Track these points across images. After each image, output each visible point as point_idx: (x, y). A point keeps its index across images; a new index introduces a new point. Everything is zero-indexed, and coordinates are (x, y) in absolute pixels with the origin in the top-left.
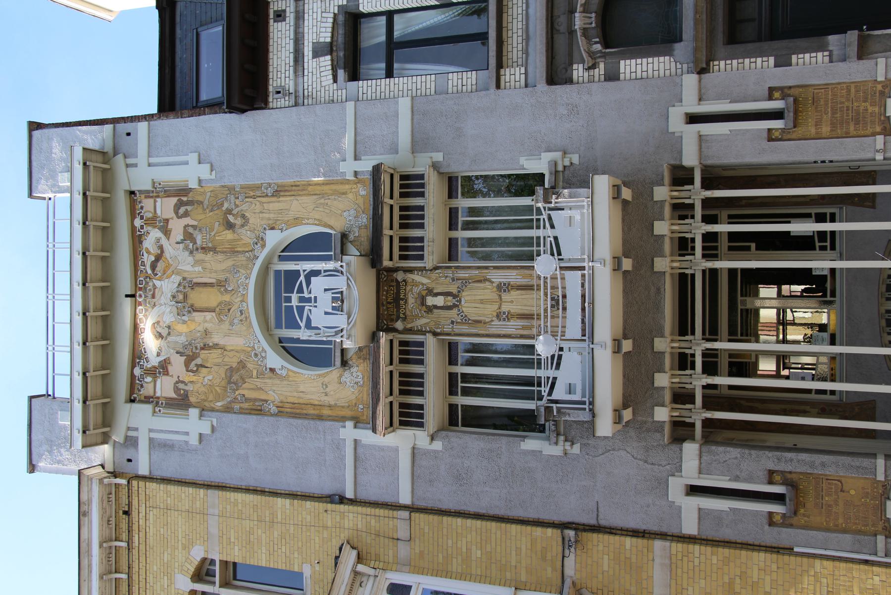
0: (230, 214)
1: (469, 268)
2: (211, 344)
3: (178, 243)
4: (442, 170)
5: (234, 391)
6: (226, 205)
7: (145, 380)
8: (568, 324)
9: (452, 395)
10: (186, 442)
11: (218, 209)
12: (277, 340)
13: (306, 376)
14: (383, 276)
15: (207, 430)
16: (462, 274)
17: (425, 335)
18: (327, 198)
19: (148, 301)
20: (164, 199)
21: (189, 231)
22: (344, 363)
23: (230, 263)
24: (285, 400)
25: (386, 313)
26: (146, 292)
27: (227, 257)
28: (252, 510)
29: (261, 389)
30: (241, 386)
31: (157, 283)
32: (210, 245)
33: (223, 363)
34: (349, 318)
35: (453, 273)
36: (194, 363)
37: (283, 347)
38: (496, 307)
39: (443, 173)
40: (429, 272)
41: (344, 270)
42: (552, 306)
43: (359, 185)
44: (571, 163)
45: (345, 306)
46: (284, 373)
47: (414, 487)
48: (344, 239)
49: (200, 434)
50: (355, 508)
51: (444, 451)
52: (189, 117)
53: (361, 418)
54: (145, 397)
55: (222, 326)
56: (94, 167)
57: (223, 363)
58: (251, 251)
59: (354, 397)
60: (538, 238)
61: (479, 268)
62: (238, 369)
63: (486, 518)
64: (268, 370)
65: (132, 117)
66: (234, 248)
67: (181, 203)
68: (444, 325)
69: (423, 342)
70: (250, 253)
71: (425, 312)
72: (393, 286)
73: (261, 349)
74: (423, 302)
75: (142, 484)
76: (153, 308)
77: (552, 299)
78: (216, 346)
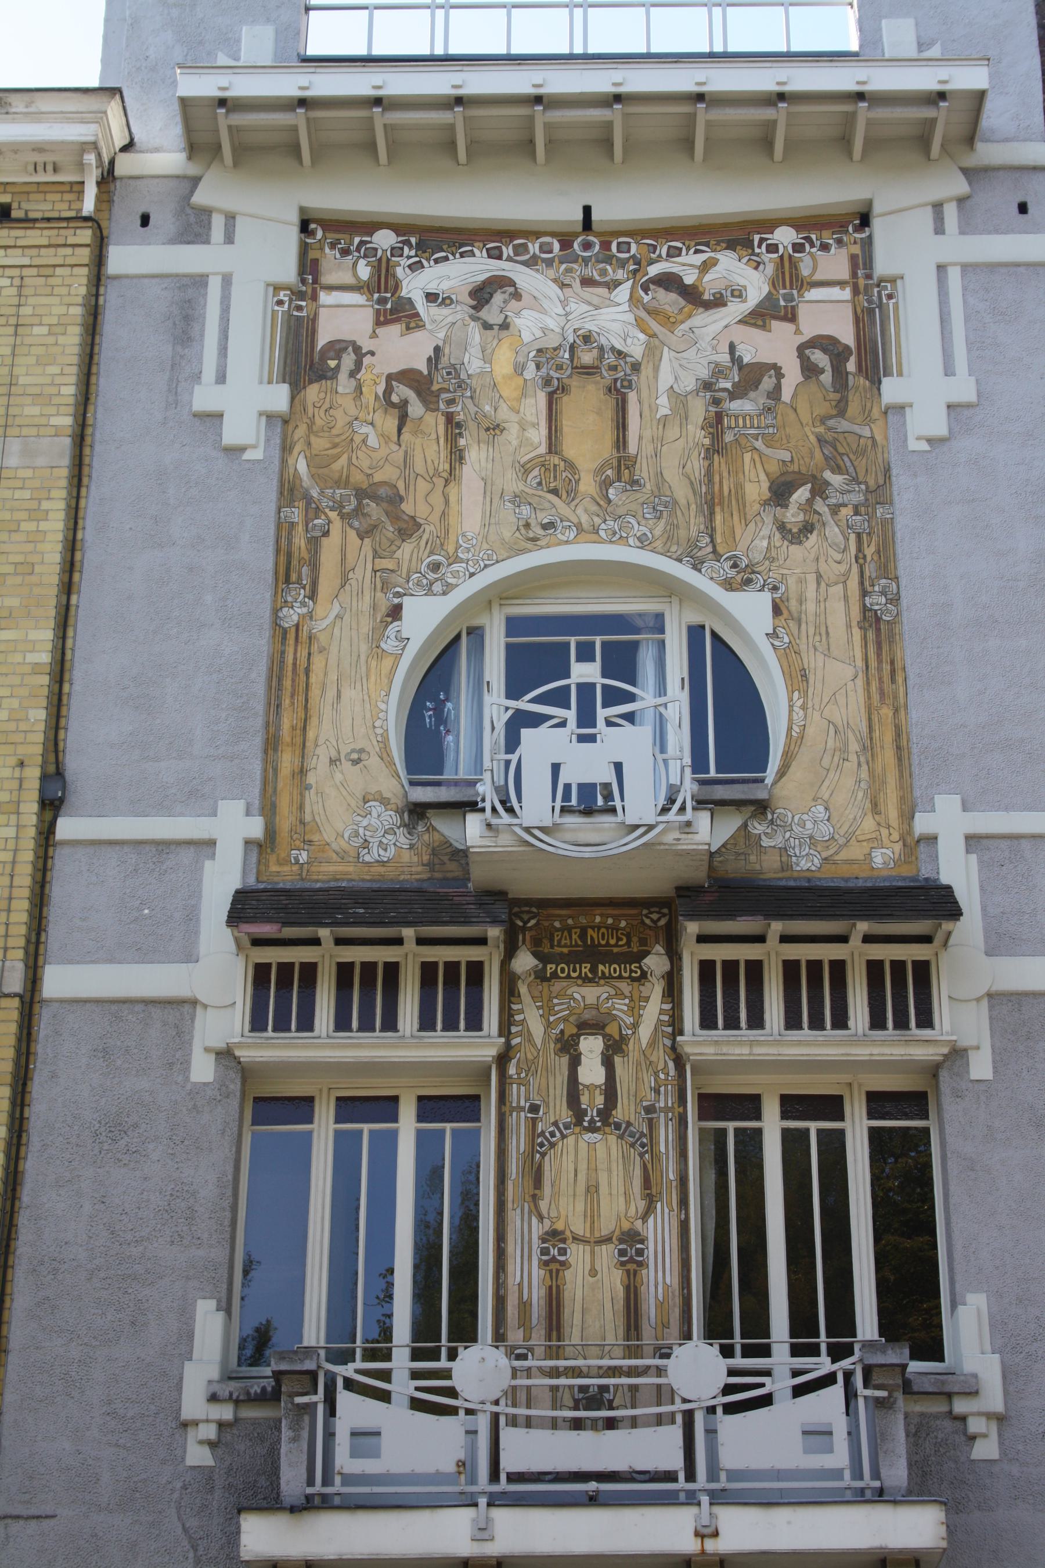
0: (814, 492)
1: (683, 1154)
2: (462, 442)
3: (732, 347)
4: (944, 1075)
5: (339, 507)
6: (836, 480)
7: (362, 262)
8: (541, 1436)
9: (337, 1106)
10: (197, 377)
11: (826, 458)
12: (476, 622)
13: (383, 706)
14: (655, 916)
15: (231, 436)
16: (665, 1136)
17: (500, 1035)
18: (862, 759)
19: (575, 266)
21: (766, 379)
22: (417, 812)
23: (682, 492)
24: (315, 648)
25: (557, 924)
26: (598, 261)
28: (20, 558)
29: (345, 581)
30: (351, 527)
31: (623, 293)
32: (728, 437)
33: (412, 475)
35: (666, 1110)
36: (410, 394)
37: (458, 637)
38: (579, 1227)
39: (935, 1076)
40: (668, 1042)
41: (672, 816)
42: (583, 1389)
43: (898, 847)
44: (973, 1438)
45: (570, 820)
46: (390, 645)
47: (88, 1005)
48: (753, 808)
49: (220, 416)
50: (31, 844)
51: (189, 1087)
53: (273, 858)
54: (315, 262)
55: (510, 474)
56: (933, 121)
57: (412, 475)
58: (715, 551)
59: (328, 835)
60: (765, 1351)
61: (683, 1180)
62: (398, 518)
63: (9, 1203)
64: (396, 601)
66: (721, 503)
67: (839, 355)
69: (480, 1029)
70: (709, 549)
71: (562, 1032)
72: (628, 944)
74: (587, 1027)
75: (84, 255)
76: (555, 281)
77: (604, 1389)
78: (457, 456)
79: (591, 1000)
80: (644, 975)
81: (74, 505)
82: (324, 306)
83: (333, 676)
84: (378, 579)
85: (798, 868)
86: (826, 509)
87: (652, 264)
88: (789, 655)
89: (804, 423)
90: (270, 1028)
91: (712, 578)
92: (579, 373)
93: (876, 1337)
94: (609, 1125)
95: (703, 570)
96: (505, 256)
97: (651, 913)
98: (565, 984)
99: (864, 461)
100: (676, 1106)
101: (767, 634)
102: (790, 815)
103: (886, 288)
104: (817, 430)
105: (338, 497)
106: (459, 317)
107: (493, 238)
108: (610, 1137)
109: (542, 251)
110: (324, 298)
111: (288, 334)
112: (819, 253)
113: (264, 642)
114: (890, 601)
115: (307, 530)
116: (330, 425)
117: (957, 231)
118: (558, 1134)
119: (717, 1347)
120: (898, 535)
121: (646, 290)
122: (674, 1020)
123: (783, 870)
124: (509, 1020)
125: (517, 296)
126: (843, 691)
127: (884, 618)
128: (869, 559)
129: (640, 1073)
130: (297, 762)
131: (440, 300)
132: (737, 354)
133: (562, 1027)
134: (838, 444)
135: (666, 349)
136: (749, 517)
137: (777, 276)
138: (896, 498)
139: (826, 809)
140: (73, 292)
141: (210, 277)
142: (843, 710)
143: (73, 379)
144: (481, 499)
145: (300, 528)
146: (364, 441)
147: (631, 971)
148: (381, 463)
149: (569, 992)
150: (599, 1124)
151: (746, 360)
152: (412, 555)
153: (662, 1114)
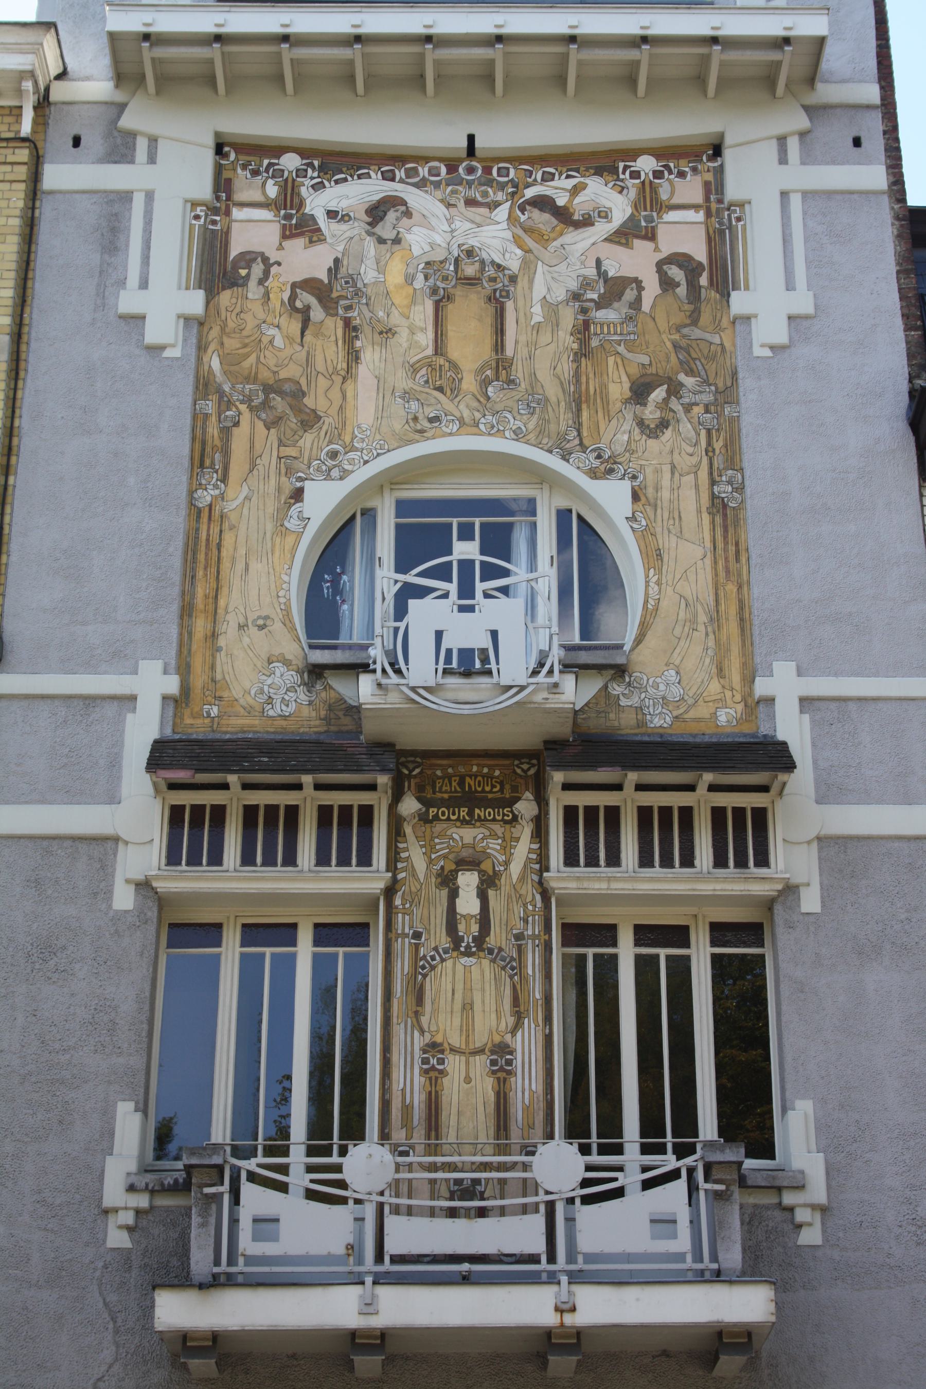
0: (669, 393)
1: (548, 976)
2: (358, 344)
3: (598, 262)
4: (778, 909)
5: (248, 400)
6: (689, 381)
7: (270, 182)
8: (420, 1223)
9: (242, 931)
10: (122, 283)
11: (681, 362)
12: (369, 504)
13: (286, 578)
14: (525, 767)
15: (153, 334)
16: (532, 960)
17: (388, 871)
19: (460, 188)
20: (701, 232)
21: (628, 291)
22: (316, 672)
23: (552, 391)
24: (226, 526)
25: (439, 773)
26: (481, 184)
27: (566, 386)
29: (253, 466)
30: (259, 418)
31: (502, 213)
32: (594, 343)
34: (426, 688)
35: (534, 937)
37: (353, 518)
38: (456, 1040)
39: (770, 909)
40: (536, 878)
41: (541, 678)
42: (458, 1182)
43: (740, 707)
44: (800, 1226)
45: (453, 681)
46: (292, 524)
47: (22, 840)
49: (143, 317)
51: (111, 914)
52: (900, 290)
53: (187, 712)
54: (229, 181)
55: (401, 373)
56: (779, 63)
58: (581, 444)
59: (236, 692)
60: (618, 1150)
62: (300, 411)
64: (298, 484)
65: (898, 149)
66: (587, 401)
67: (693, 270)
68: (411, 914)
69: (370, 865)
70: (577, 442)
71: (442, 868)
72: (502, 790)
73: (347, 467)
75: (22, 172)
76: (442, 201)
77: (476, 1182)
78: (354, 356)
79: (468, 840)
80: (515, 818)
81: (11, 396)
82: (236, 221)
83: (242, 551)
84: (282, 465)
85: (652, 725)
86: (680, 408)
87: (528, 187)
88: (645, 536)
89: (662, 331)
90: (184, 862)
91: (578, 468)
92: (463, 284)
93: (716, 1137)
94: (483, 950)
95: (571, 460)
96: (397, 179)
97: (522, 763)
98: (445, 826)
99: (714, 365)
100: (542, 933)
101: (627, 518)
102: (645, 678)
103: (735, 212)
104: (673, 337)
105: (247, 392)
106: (356, 232)
107: (387, 162)
108: (483, 961)
109: (430, 174)
110: (236, 213)
111: (204, 245)
112: (677, 179)
113: (181, 520)
114: (735, 490)
115: (220, 421)
116: (241, 327)
117: (799, 162)
118: (438, 958)
119: (576, 1146)
120: (744, 431)
121: (523, 210)
122: (541, 859)
123: (638, 726)
124: (395, 857)
125: (408, 214)
126: (693, 569)
127: (730, 504)
128: (717, 452)
129: (511, 905)
130: (209, 626)
131: (340, 216)
132: (603, 268)
133: (442, 863)
134: (691, 350)
135: (540, 263)
136: (612, 413)
137: (639, 199)
138: (742, 399)
139: (677, 673)
140: (12, 205)
141: (135, 193)
142: (693, 586)
143: (11, 283)
144: (375, 394)
145: (214, 419)
146: (271, 342)
147: (504, 815)
148: (286, 362)
149: (449, 833)
150: (474, 949)
151: (610, 274)
152: (312, 444)
153: (530, 941)
